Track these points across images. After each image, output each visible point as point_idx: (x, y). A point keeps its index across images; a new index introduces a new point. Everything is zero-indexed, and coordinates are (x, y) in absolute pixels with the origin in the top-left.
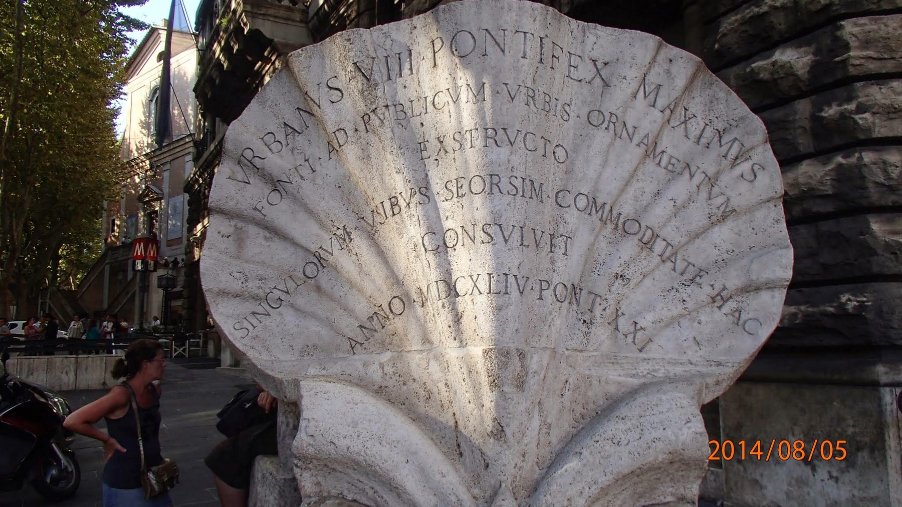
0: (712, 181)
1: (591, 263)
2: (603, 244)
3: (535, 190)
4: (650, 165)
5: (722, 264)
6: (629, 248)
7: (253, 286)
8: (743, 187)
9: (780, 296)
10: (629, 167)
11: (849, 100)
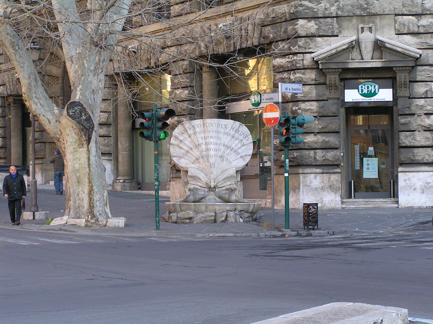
0: (241, 141)
1: (224, 152)
2: (225, 150)
3: (217, 144)
4: (233, 139)
5: (242, 152)
6: (229, 150)
7: (178, 155)
8: (246, 141)
9: (250, 157)
10: (229, 140)
11: (297, 106)
